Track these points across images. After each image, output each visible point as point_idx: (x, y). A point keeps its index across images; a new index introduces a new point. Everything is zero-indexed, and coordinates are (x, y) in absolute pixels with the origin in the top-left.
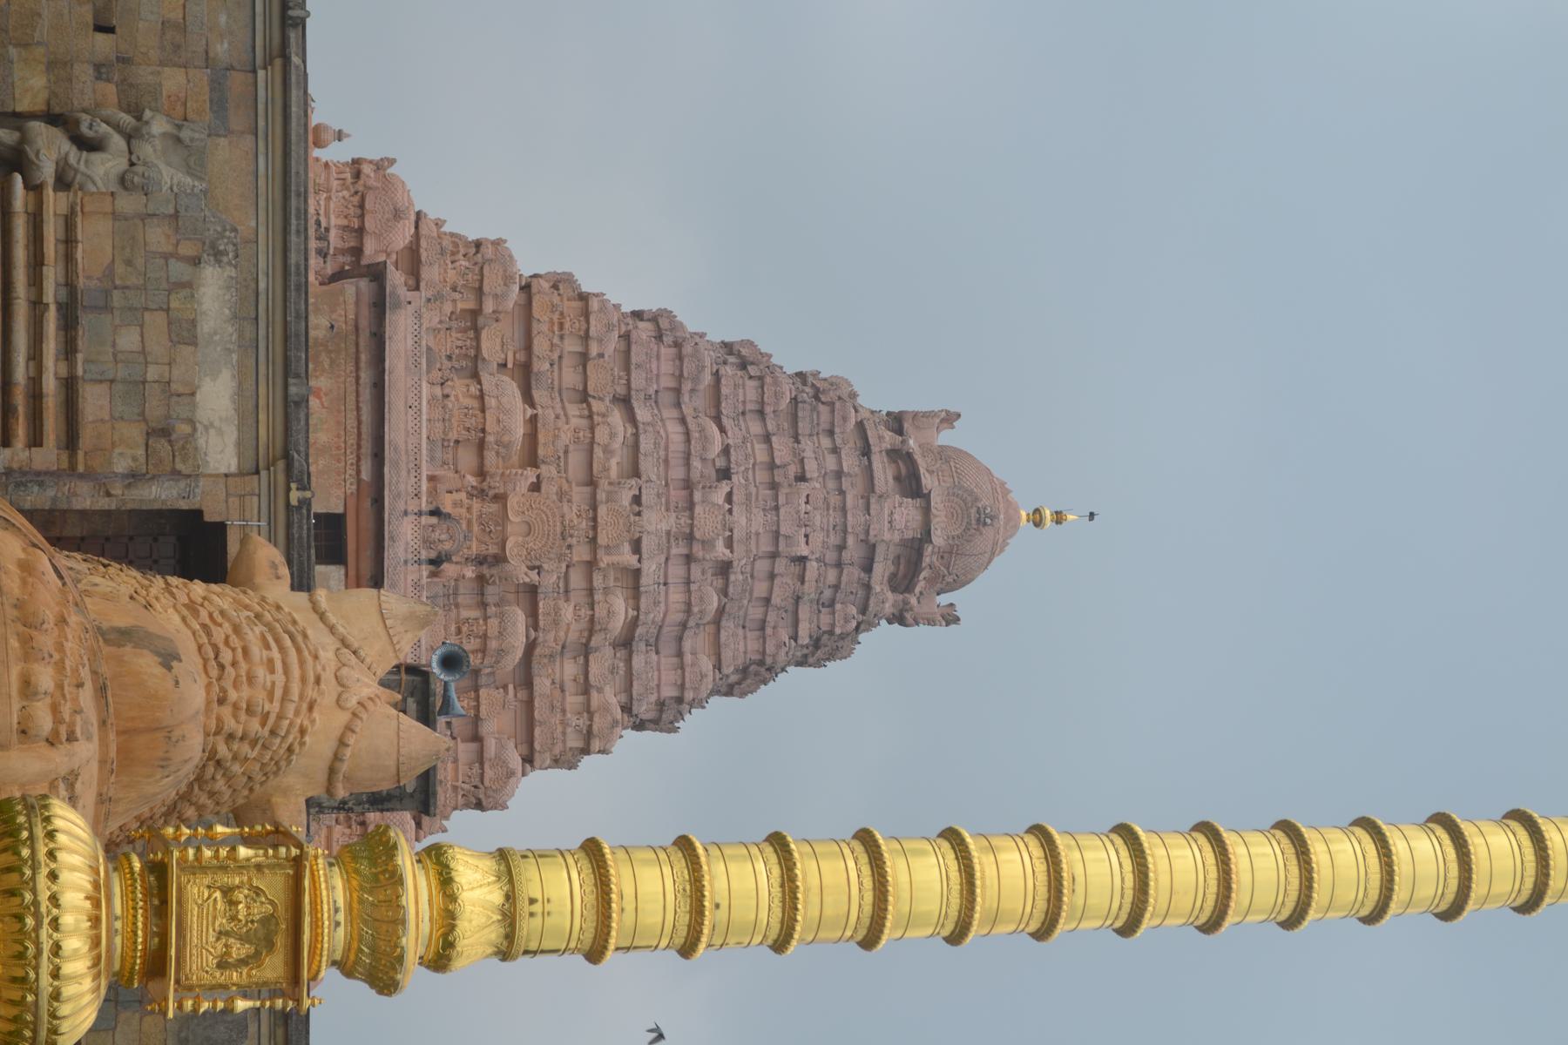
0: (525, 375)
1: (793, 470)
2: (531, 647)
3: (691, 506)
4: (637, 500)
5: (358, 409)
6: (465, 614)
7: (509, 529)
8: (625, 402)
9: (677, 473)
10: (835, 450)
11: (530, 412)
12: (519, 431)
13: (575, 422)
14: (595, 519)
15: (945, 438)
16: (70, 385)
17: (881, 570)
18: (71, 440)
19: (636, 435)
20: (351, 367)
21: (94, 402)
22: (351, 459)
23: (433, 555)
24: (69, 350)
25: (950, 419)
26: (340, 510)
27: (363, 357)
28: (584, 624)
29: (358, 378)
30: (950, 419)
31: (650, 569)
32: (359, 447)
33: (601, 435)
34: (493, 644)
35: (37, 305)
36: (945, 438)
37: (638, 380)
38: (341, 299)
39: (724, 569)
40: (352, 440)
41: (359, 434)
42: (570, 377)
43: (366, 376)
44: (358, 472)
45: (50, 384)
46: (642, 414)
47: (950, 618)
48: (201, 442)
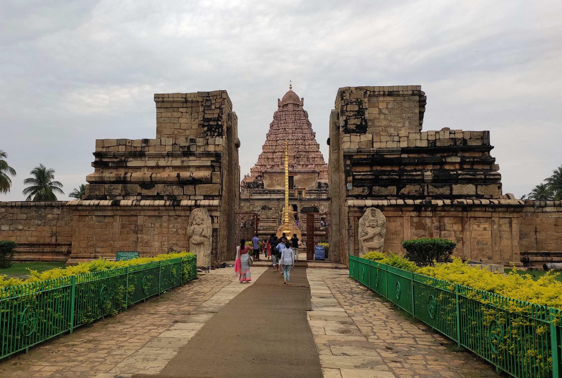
0: (274, 152)
1: (285, 120)
8: (277, 141)
16: (273, 218)
21: (274, 217)
24: (270, 218)
25: (279, 100)
30: (279, 100)
35: (268, 220)
36: (281, 100)
45: (273, 220)
46: (278, 139)
47: (303, 99)
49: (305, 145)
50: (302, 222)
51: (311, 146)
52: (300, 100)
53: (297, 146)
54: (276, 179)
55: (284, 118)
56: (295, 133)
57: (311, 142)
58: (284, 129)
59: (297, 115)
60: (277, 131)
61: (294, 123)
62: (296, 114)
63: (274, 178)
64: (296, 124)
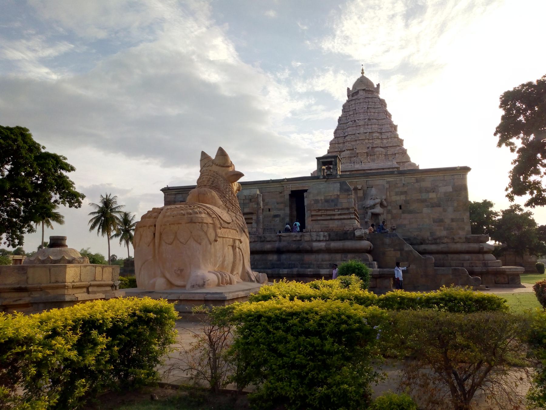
1: (354, 111)
2: (381, 147)
3: (360, 126)
4: (359, 134)
6: (376, 157)
7: (362, 152)
8: (345, 137)
9: (355, 128)
10: (352, 105)
11: (346, 151)
12: (348, 152)
13: (347, 144)
15: (351, 89)
17: (370, 96)
18: (251, 213)
19: (349, 135)
23: (360, 162)
28: (378, 140)
31: (369, 131)
33: (349, 140)
34: (380, 153)
37: (341, 135)
39: (369, 119)
42: (341, 145)
46: (346, 134)
48: (252, 194)
49: (382, 139)
50: (310, 219)
51: (390, 140)
52: (376, 86)
53: (371, 141)
55: (354, 108)
56: (367, 125)
57: (390, 135)
58: (353, 122)
59: (370, 103)
60: (344, 125)
61: (367, 112)
62: (369, 102)
64: (369, 114)
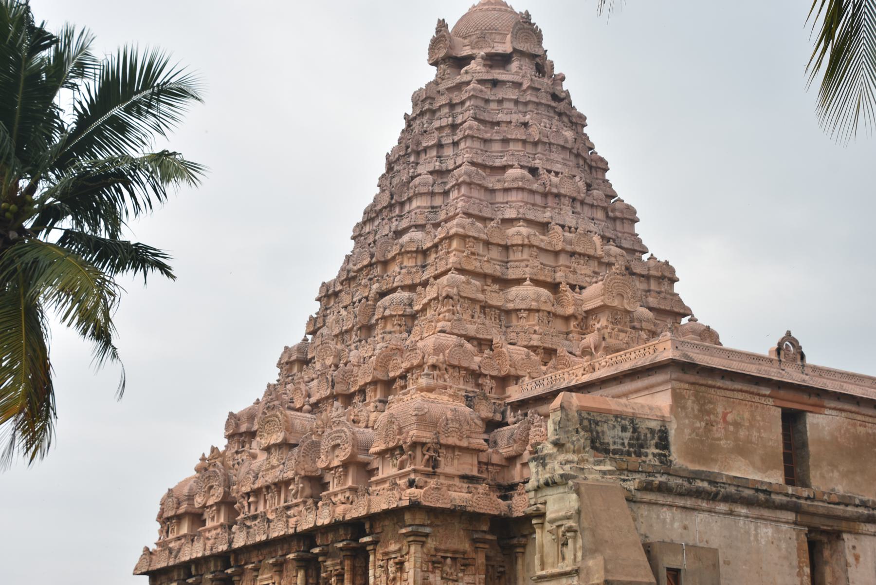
5: (733, 390)
14: (580, 254)
20: (712, 391)
22: (757, 399)
25: (442, 25)
26: (780, 410)
27: (710, 382)
29: (719, 388)
32: (752, 393)
38: (678, 391)
40: (748, 397)
41: (746, 392)
43: (719, 383)
44: (764, 396)
54: (730, 418)
63: (720, 410)
